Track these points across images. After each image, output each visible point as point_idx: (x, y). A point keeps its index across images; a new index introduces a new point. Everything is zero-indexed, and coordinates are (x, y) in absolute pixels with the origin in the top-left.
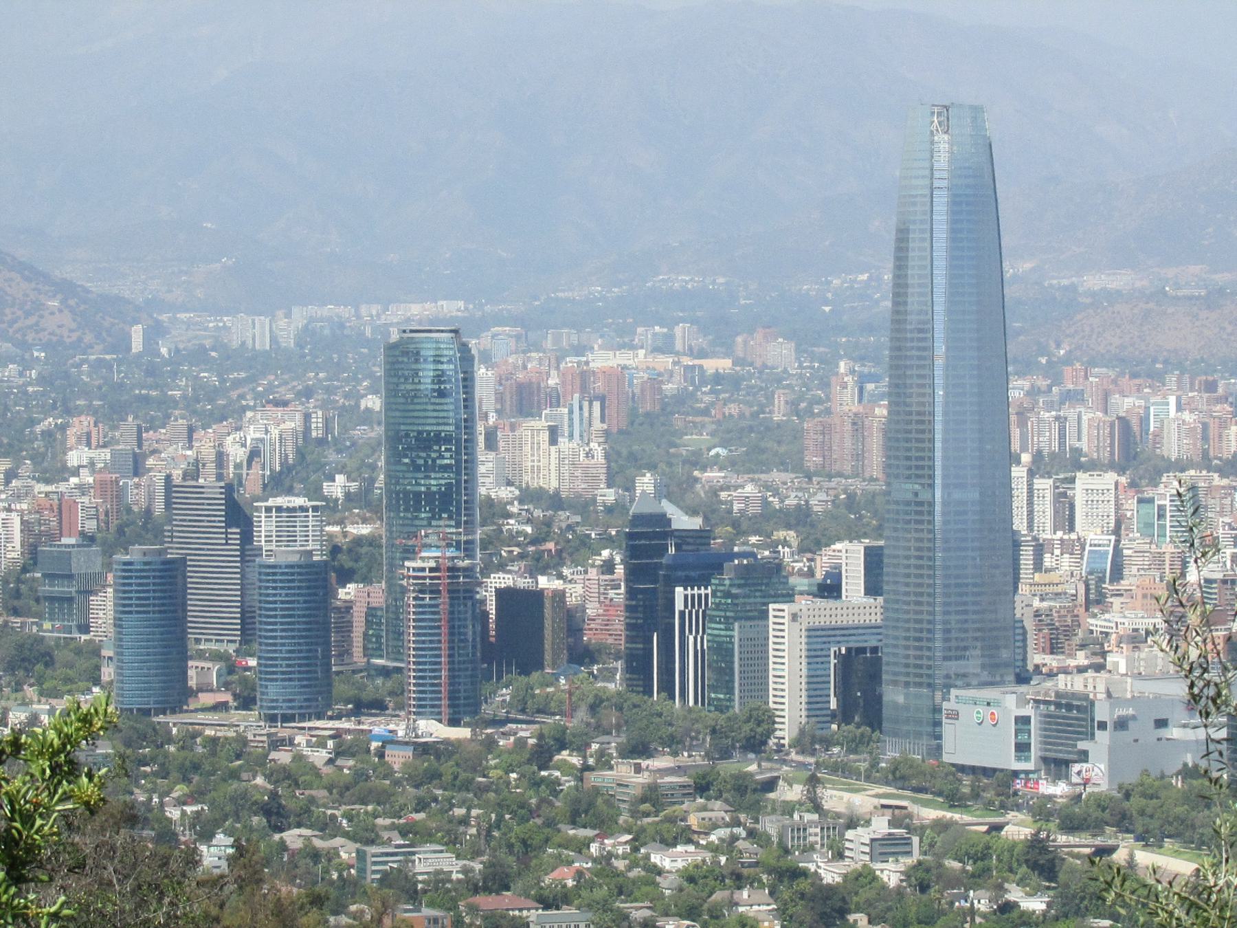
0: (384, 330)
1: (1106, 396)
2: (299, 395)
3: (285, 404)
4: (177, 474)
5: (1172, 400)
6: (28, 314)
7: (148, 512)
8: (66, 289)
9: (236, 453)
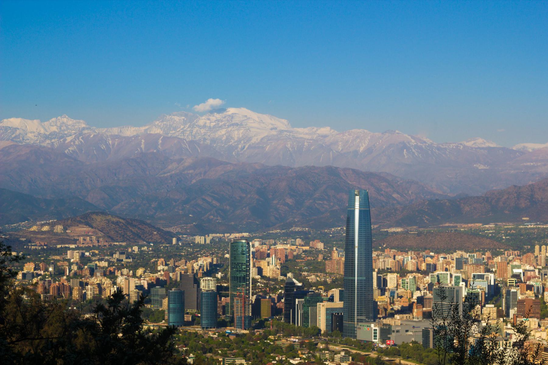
0: (230, 240)
1: (394, 256)
2: (211, 254)
3: (207, 256)
4: (183, 272)
5: (410, 257)
6: (149, 235)
7: (176, 280)
8: (158, 230)
9: (196, 267)
